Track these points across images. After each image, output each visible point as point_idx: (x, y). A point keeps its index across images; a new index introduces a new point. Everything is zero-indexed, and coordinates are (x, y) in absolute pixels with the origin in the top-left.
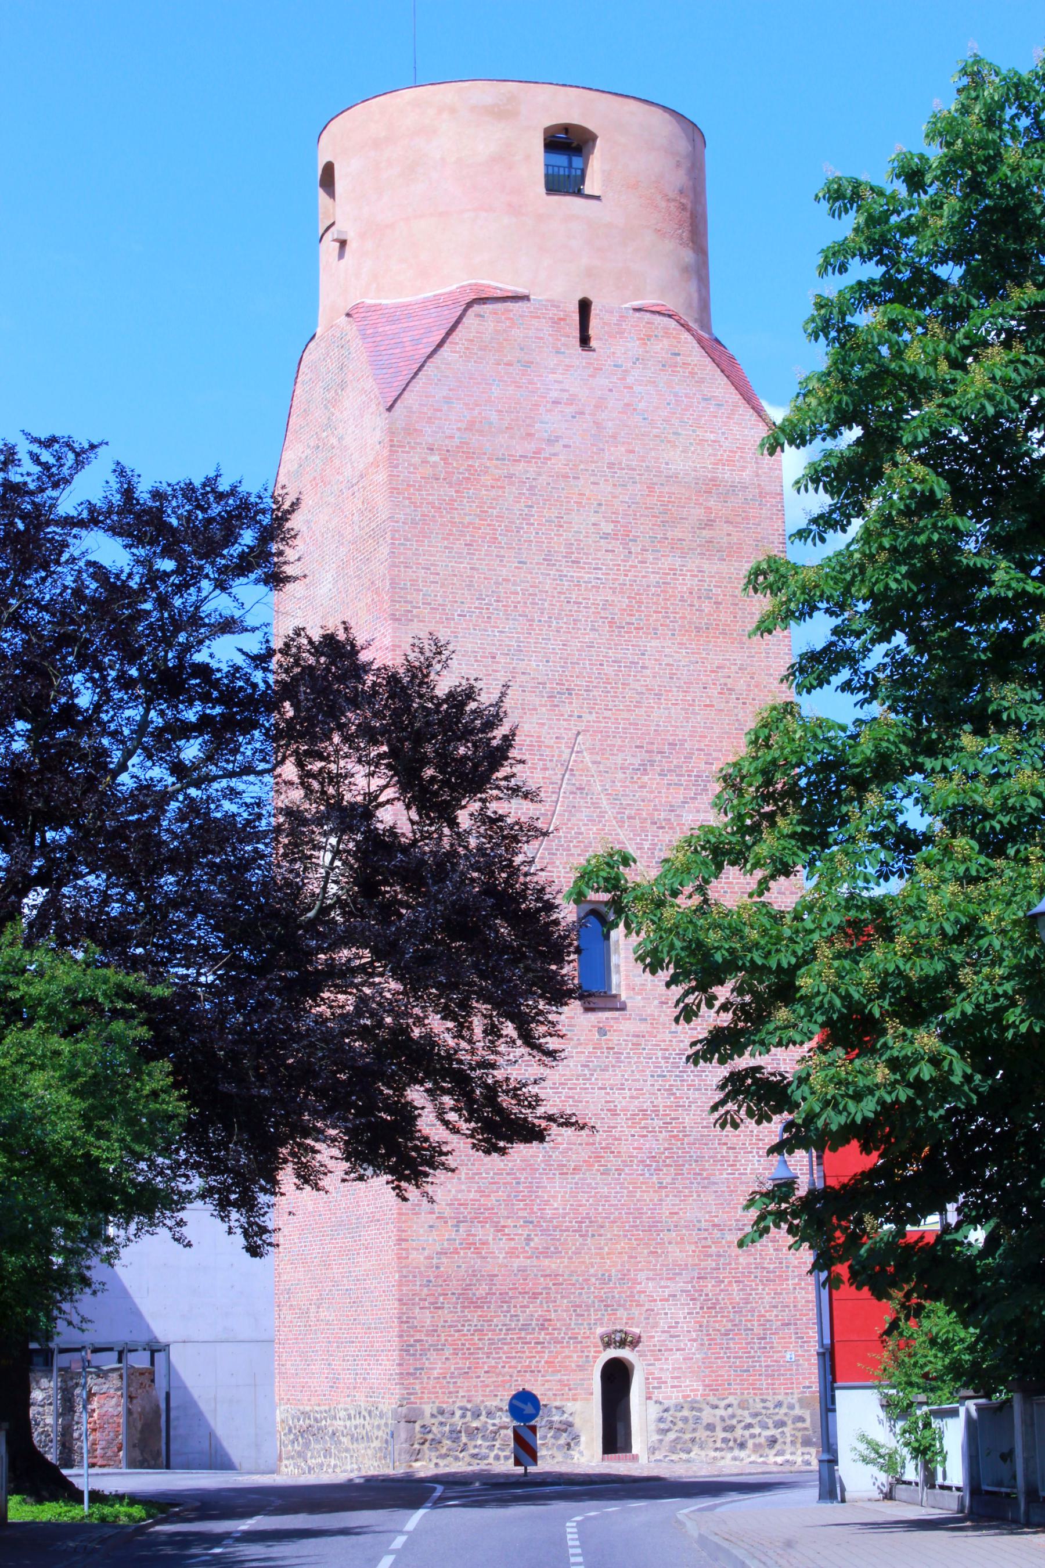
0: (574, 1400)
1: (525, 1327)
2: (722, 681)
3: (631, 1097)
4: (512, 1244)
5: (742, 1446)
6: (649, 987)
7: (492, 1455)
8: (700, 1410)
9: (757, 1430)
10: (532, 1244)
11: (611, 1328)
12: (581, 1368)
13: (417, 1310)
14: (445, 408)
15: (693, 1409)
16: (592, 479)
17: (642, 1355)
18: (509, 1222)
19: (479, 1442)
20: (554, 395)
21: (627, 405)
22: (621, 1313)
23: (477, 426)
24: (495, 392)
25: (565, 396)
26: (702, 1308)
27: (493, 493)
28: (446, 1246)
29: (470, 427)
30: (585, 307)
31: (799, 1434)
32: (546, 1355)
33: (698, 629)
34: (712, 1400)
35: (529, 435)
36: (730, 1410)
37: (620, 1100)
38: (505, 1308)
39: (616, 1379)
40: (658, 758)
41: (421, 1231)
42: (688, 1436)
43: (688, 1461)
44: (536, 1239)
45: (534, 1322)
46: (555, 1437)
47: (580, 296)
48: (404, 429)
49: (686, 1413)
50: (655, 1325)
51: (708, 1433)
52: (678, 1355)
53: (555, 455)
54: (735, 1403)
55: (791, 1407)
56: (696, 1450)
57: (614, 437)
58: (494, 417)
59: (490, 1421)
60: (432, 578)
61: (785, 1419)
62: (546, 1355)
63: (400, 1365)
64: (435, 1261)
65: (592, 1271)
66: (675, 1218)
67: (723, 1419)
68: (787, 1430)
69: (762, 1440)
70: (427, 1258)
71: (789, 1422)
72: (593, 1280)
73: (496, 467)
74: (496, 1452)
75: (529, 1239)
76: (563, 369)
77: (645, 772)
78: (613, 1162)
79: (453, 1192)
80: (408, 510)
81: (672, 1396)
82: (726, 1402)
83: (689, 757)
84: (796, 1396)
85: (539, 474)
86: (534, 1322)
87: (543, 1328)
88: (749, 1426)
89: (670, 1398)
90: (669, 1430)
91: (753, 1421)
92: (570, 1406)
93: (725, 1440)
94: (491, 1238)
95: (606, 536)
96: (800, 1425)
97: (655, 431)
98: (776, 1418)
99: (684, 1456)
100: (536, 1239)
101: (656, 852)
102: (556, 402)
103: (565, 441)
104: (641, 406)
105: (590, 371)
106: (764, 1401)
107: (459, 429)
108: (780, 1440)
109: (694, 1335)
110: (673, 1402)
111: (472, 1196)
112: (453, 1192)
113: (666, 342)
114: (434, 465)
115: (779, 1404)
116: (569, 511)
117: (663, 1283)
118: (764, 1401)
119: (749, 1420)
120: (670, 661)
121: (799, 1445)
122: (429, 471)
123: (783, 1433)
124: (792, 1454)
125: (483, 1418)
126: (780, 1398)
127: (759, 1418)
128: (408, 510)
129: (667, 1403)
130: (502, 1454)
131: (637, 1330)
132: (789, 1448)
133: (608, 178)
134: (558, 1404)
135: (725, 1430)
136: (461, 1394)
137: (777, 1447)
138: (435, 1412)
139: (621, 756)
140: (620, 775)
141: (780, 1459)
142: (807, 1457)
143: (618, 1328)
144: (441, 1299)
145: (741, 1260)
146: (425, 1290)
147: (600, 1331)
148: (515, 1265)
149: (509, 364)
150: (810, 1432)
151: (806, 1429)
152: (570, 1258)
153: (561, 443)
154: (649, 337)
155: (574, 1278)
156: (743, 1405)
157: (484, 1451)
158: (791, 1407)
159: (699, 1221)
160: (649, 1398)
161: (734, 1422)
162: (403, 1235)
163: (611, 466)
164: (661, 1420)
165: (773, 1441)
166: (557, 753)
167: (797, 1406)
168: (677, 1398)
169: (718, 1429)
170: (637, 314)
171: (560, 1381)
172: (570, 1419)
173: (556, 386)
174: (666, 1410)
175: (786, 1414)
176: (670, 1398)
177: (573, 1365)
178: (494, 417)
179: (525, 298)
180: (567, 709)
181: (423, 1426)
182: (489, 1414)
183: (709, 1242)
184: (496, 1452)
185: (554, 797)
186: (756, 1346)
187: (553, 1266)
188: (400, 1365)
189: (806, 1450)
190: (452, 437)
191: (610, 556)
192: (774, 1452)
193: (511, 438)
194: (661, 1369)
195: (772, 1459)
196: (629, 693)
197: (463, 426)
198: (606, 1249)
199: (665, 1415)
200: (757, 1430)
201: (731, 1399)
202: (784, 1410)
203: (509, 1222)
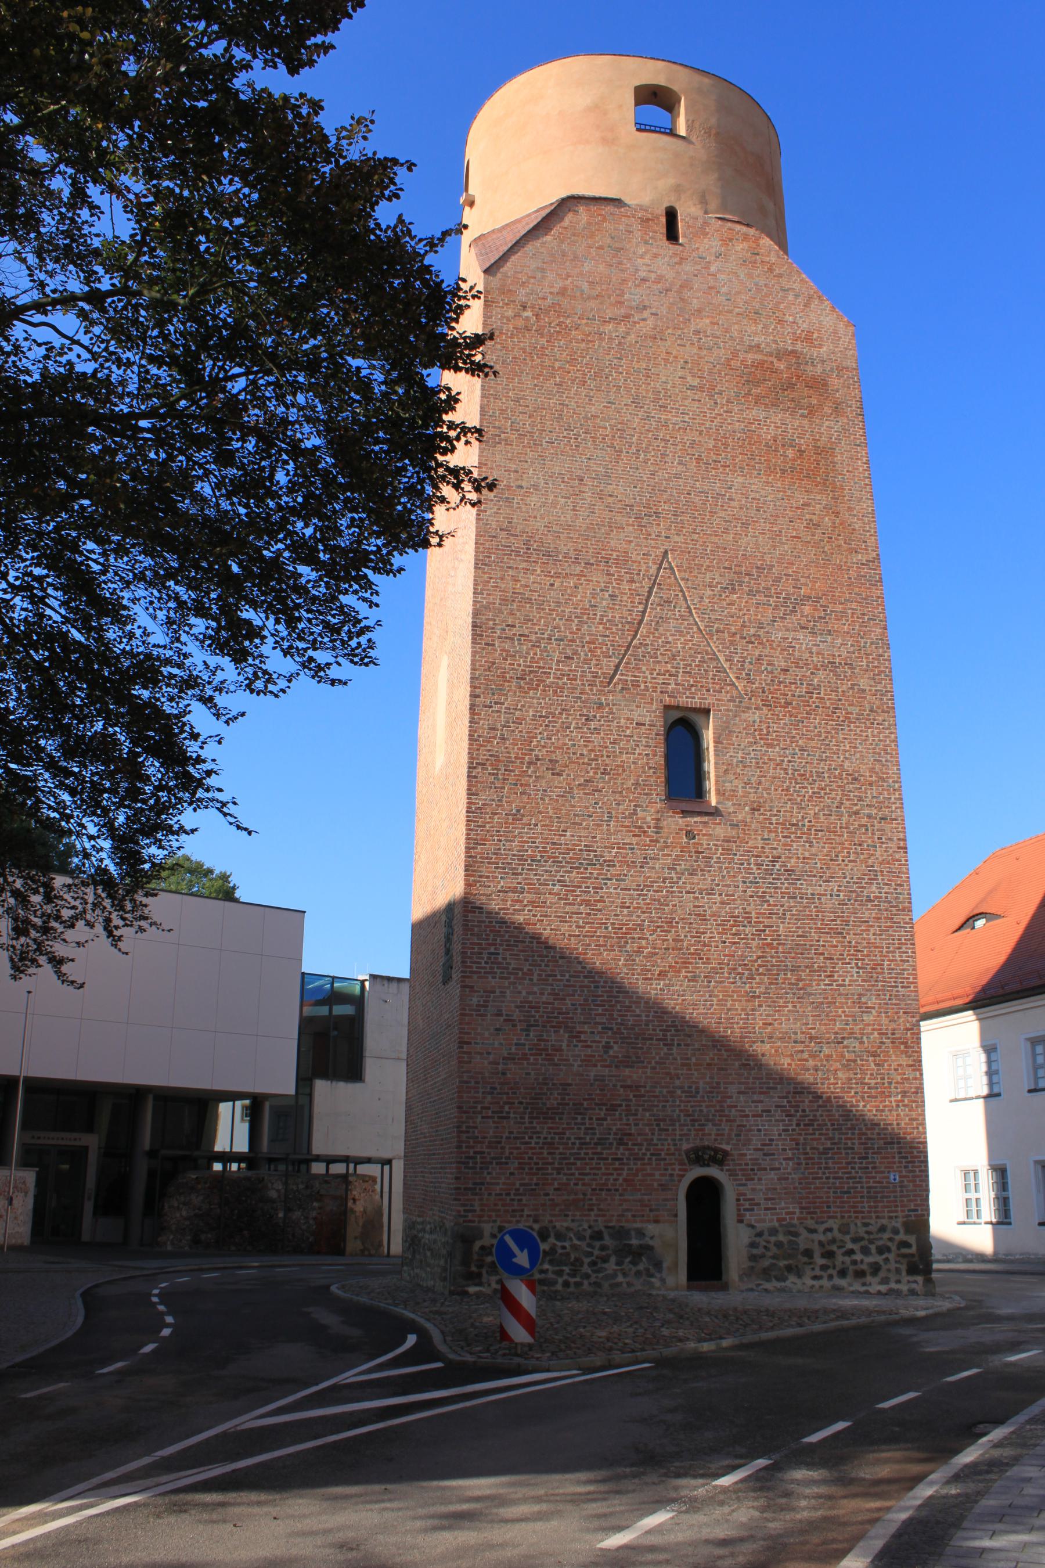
0: (657, 1221)
1: (601, 1142)
2: (807, 516)
3: (722, 903)
4: (589, 1051)
5: (843, 1273)
6: (740, 793)
7: (560, 1280)
8: (796, 1234)
9: (858, 1257)
10: (611, 1053)
11: (698, 1143)
12: (663, 1187)
13: (479, 1119)
14: (539, 275)
15: (791, 1233)
16: (679, 342)
17: (732, 1174)
18: (586, 1028)
19: (546, 1266)
20: (642, 274)
21: (710, 288)
22: (709, 1128)
23: (569, 292)
24: (587, 267)
25: (653, 276)
26: (798, 1125)
27: (583, 345)
28: (513, 1050)
29: (563, 292)
30: (671, 215)
31: (905, 1261)
32: (625, 1172)
33: (783, 471)
34: (810, 1223)
35: (619, 302)
36: (829, 1235)
37: (712, 905)
38: (579, 1120)
39: (705, 1200)
40: (747, 579)
41: (487, 1034)
42: (782, 1263)
43: (782, 1290)
44: (616, 1047)
45: (611, 1137)
46: (634, 1263)
47: (666, 204)
48: (499, 289)
49: (781, 1237)
50: (748, 1142)
51: (805, 1259)
52: (773, 1175)
53: (644, 320)
54: (835, 1227)
55: (896, 1231)
56: (792, 1278)
57: (699, 311)
58: (585, 286)
59: (559, 1244)
60: (521, 409)
61: (889, 1244)
62: (625, 1172)
63: (457, 1178)
64: (500, 1067)
65: (677, 1083)
66: (769, 1029)
67: (821, 1244)
68: (891, 1257)
69: (864, 1267)
70: (490, 1063)
71: (894, 1248)
72: (679, 1092)
73: (587, 325)
74: (565, 1277)
75: (607, 1047)
76: (653, 257)
77: (734, 591)
78: (703, 969)
79: (524, 993)
80: (499, 353)
81: (766, 1220)
82: (826, 1226)
83: (778, 580)
84: (900, 1220)
85: (628, 334)
86: (611, 1137)
87: (621, 1142)
88: (851, 1252)
89: (764, 1221)
90: (763, 1256)
91: (856, 1247)
92: (651, 1229)
93: (824, 1268)
94: (564, 1045)
95: (692, 388)
96: (905, 1251)
97: (737, 310)
98: (880, 1243)
99: (779, 1285)
100: (616, 1047)
101: (746, 665)
102: (644, 280)
103: (654, 310)
104: (723, 290)
105: (677, 259)
106: (866, 1225)
107: (551, 293)
108: (884, 1267)
109: (790, 1154)
110: (767, 1225)
111: (544, 998)
112: (524, 993)
113: (745, 245)
114: (527, 319)
115: (883, 1229)
116: (656, 365)
117: (755, 1097)
118: (866, 1225)
119: (850, 1246)
120: (757, 496)
121: (904, 1273)
122: (521, 323)
123: (887, 1260)
124: (898, 1282)
125: (552, 1240)
126: (884, 1222)
127: (862, 1243)
128: (499, 353)
129: (760, 1226)
130: (572, 1280)
131: (727, 1148)
132: (893, 1277)
133: (690, 127)
134: (638, 1225)
135: (823, 1256)
136: (526, 1212)
137: (882, 1274)
138: (495, 1231)
139: (709, 575)
140: (709, 592)
141: (883, 1288)
142: (914, 1286)
144: (507, 1108)
145: (840, 1074)
146: (489, 1098)
147: (685, 1146)
148: (592, 1074)
149: (601, 248)
150: (916, 1259)
151: (912, 1255)
152: (654, 1068)
153: (649, 311)
154: (731, 240)
155: (658, 1090)
156: (844, 1230)
157: (550, 1275)
158: (896, 1231)
159: (796, 1033)
160: (740, 1221)
161: (834, 1248)
162: (466, 1038)
163: (697, 332)
164: (753, 1245)
165: (876, 1269)
166: (643, 568)
167: (902, 1231)
168: (771, 1220)
169: (817, 1255)
170: (720, 222)
171: (640, 1201)
172: (651, 1243)
173: (644, 268)
174: (760, 1234)
175: (891, 1239)
176: (764, 1221)
177: (655, 1184)
178: (585, 286)
179: (616, 202)
180: (654, 530)
181: (482, 1248)
182: (559, 1236)
183: (805, 1055)
184: (565, 1277)
185: (641, 608)
186: (857, 1166)
187: (635, 1076)
188: (457, 1178)
189: (911, 1278)
190: (544, 299)
191: (697, 404)
192: (877, 1279)
193: (601, 303)
194: (753, 1190)
195: (876, 1287)
196: (716, 521)
197: (555, 290)
198: (694, 1060)
199: (757, 1239)
200: (858, 1257)
201: (831, 1223)
202: (886, 1236)
203: (586, 1028)
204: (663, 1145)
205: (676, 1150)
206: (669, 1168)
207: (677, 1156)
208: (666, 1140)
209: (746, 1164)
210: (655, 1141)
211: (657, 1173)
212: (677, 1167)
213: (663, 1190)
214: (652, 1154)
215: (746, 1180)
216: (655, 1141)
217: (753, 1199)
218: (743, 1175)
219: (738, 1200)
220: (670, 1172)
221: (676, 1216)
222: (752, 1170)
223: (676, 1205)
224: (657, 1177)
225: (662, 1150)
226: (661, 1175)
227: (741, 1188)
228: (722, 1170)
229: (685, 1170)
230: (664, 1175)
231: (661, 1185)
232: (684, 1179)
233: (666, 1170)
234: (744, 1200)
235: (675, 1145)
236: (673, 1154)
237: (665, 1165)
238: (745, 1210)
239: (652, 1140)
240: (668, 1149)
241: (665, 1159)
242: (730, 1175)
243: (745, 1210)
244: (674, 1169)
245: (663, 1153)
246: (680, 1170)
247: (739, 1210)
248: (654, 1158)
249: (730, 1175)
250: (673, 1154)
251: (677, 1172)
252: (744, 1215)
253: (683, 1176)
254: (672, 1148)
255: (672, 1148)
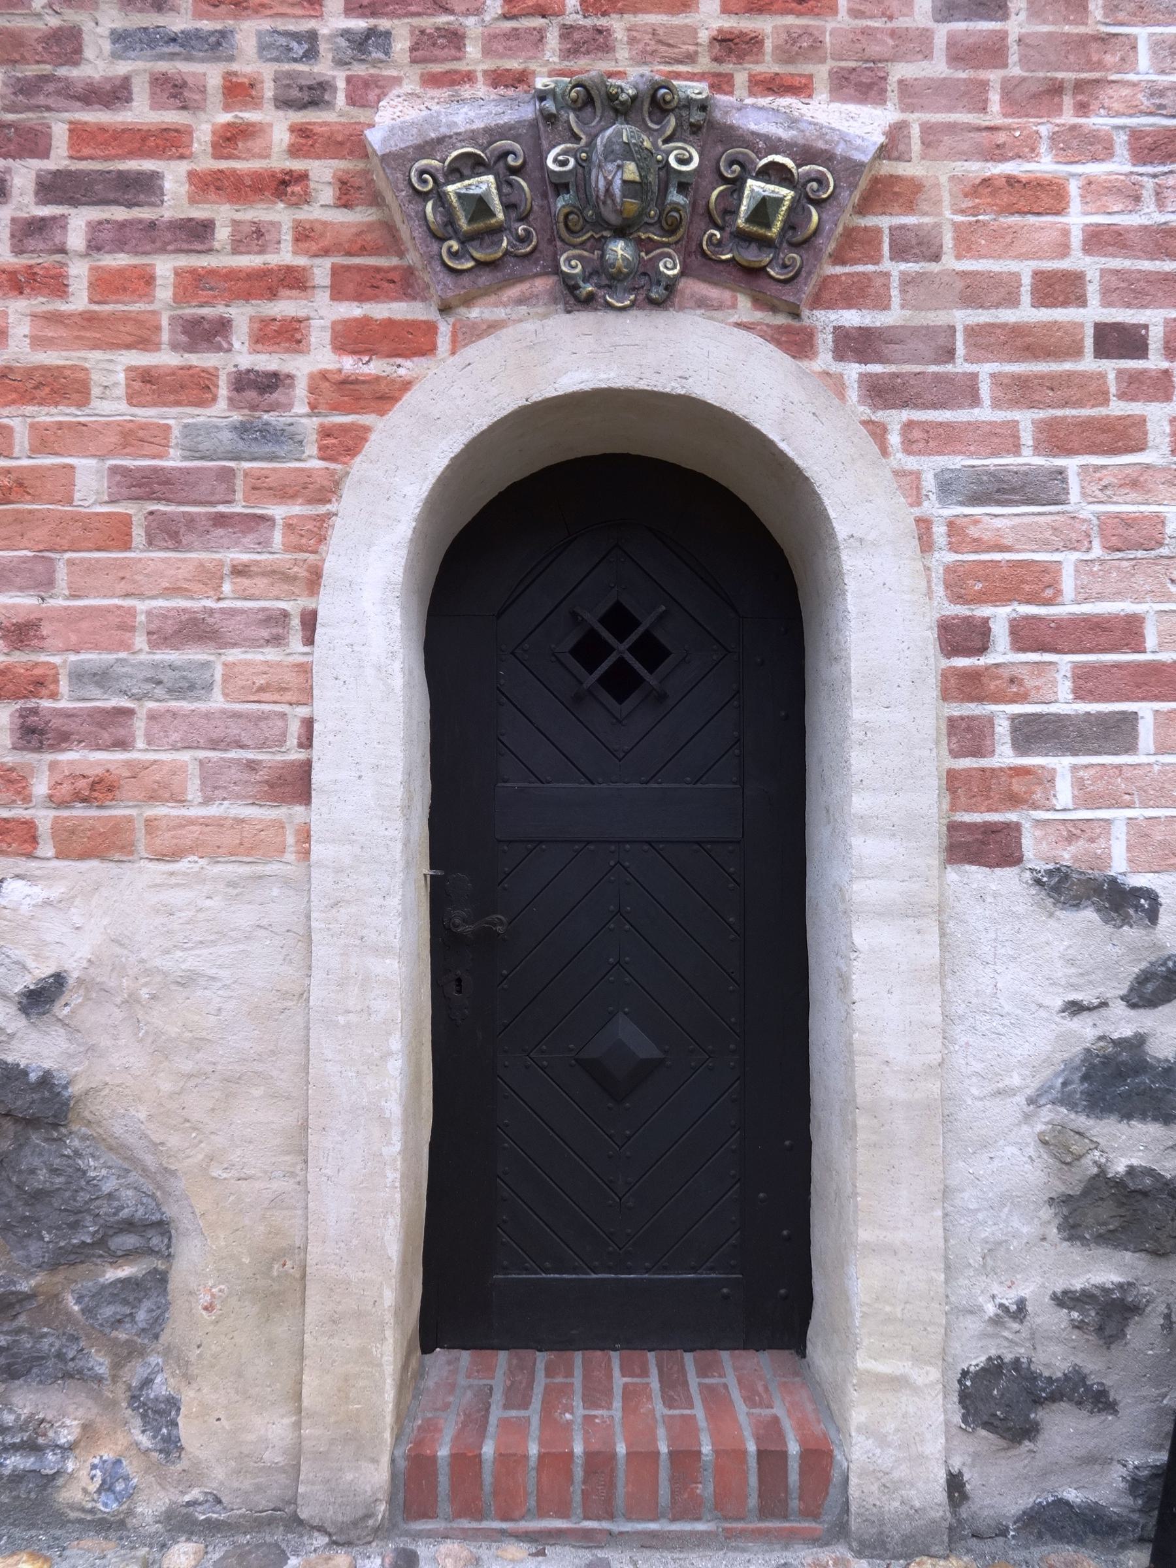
17: (899, 382)
131: (859, 126)
143: (629, 73)
177: (90, 482)
204: (173, 91)
205: (306, 141)
206: (241, 315)
207: (322, 208)
208: (216, 45)
209: (1058, 288)
210: (97, 64)
211: (111, 369)
212: (324, 312)
213: (167, 533)
214: (55, 188)
215: (1056, 439)
216: (97, 64)
217: (1128, 632)
218: (1019, 391)
219: (962, 637)
220: (243, 355)
221: (296, 784)
222: (1119, 341)
223: (302, 683)
224: (111, 406)
225: (170, 142)
226: (148, 385)
227: (999, 519)
228: (798, 344)
229: (413, 341)
230: (194, 388)
231: (146, 485)
232: (387, 431)
233: (206, 334)
234: (1027, 636)
235: (315, 95)
236: (284, 185)
237: (194, 284)
238: (1035, 733)
239: (66, 45)
240: (230, 139)
241: (197, 233)
242: (880, 393)
243: (1035, 733)
244: (288, 335)
245: (174, 177)
246: (354, 338)
247: (968, 736)
248: (79, 222)
249: (880, 393)
250: (284, 185)
251: (319, 357)
252: (1019, 788)
253: (383, 396)
254: (279, 128)
255: (279, 128)
